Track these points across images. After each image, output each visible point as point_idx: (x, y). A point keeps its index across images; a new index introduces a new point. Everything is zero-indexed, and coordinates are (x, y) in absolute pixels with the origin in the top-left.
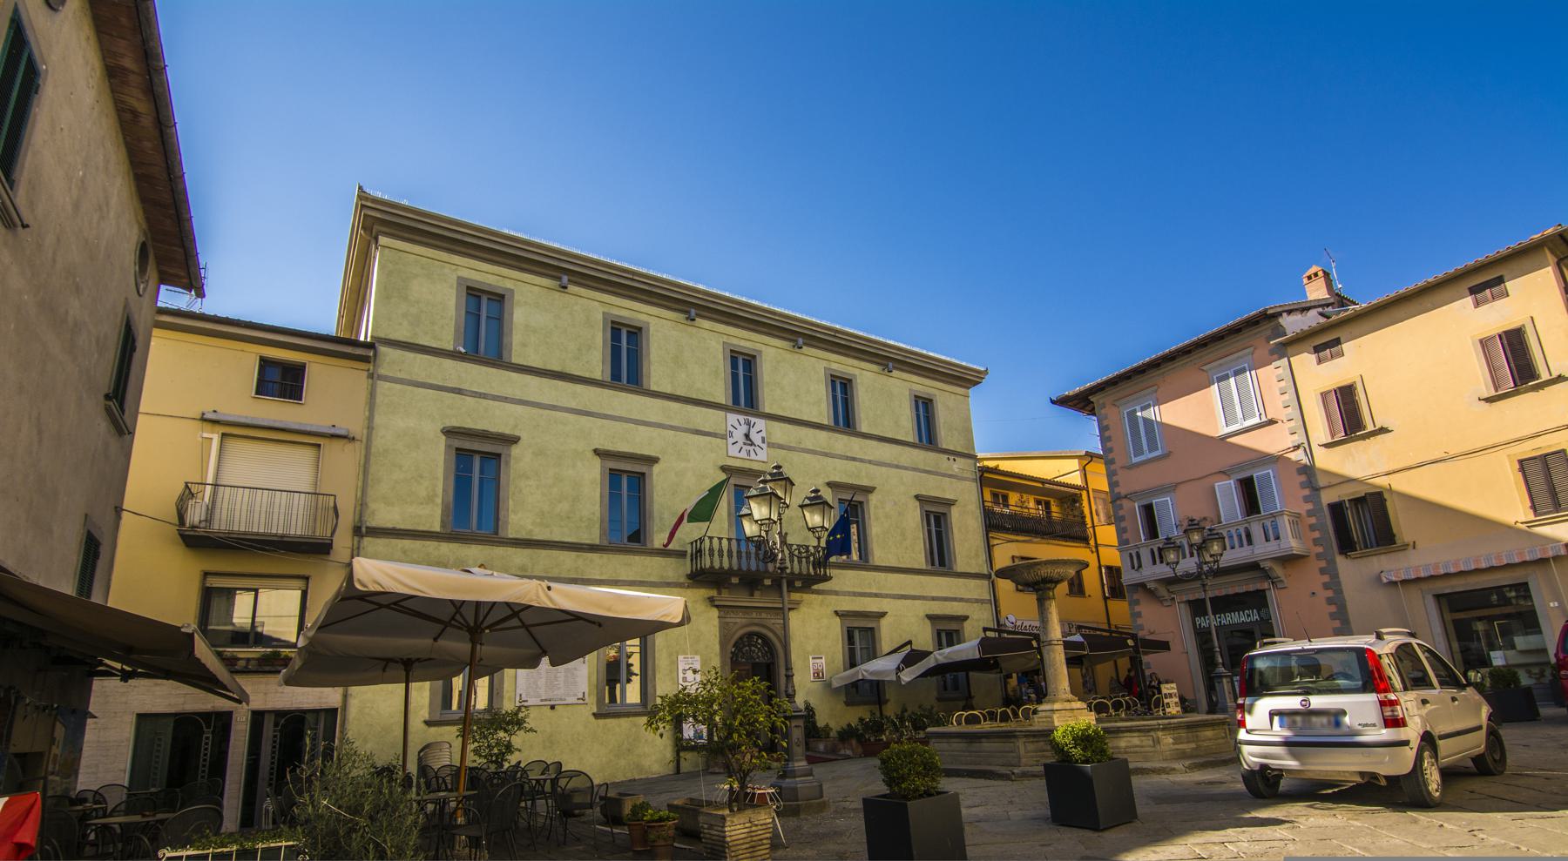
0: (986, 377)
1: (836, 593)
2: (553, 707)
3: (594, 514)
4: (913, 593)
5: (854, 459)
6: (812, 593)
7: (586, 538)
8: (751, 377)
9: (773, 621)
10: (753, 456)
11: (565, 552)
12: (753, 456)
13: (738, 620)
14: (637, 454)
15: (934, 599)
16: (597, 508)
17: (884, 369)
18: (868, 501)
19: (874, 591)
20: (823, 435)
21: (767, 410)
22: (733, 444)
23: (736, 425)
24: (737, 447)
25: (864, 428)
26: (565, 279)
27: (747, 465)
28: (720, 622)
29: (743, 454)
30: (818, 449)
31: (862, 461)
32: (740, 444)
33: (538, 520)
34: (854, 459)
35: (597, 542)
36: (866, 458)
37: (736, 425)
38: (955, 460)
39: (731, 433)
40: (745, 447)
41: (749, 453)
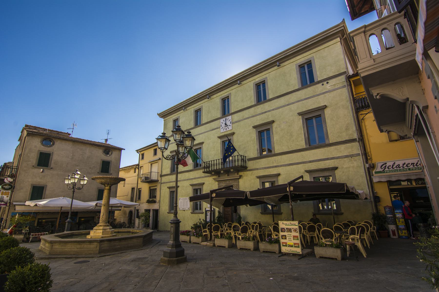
2: (184, 210)
4: (297, 162)
6: (248, 171)
9: (233, 183)
10: (228, 130)
12: (228, 130)
13: (223, 185)
14: (198, 143)
15: (310, 162)
19: (275, 165)
29: (225, 130)
32: (224, 127)
34: (266, 112)
41: (226, 129)
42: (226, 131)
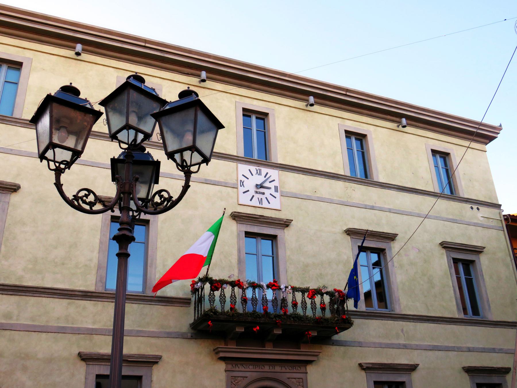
0: (501, 132)
1: (360, 344)
3: (91, 260)
5: (372, 208)
6: (333, 344)
7: (79, 285)
8: (265, 132)
10: (265, 204)
11: (57, 300)
13: (247, 374)
16: (95, 255)
17: (398, 126)
18: (390, 248)
19: (402, 342)
20: (339, 184)
21: (280, 161)
22: (244, 193)
23: (248, 175)
24: (249, 195)
25: (382, 178)
26: (79, 47)
27: (259, 212)
28: (227, 377)
29: (255, 202)
30: (335, 198)
31: (381, 210)
32: (252, 192)
33: (30, 266)
34: (372, 208)
35: (92, 289)
36: (387, 206)
37: (248, 175)
38: (478, 209)
39: (242, 183)
40: (257, 196)
41: (261, 201)
42: (261, 206)
